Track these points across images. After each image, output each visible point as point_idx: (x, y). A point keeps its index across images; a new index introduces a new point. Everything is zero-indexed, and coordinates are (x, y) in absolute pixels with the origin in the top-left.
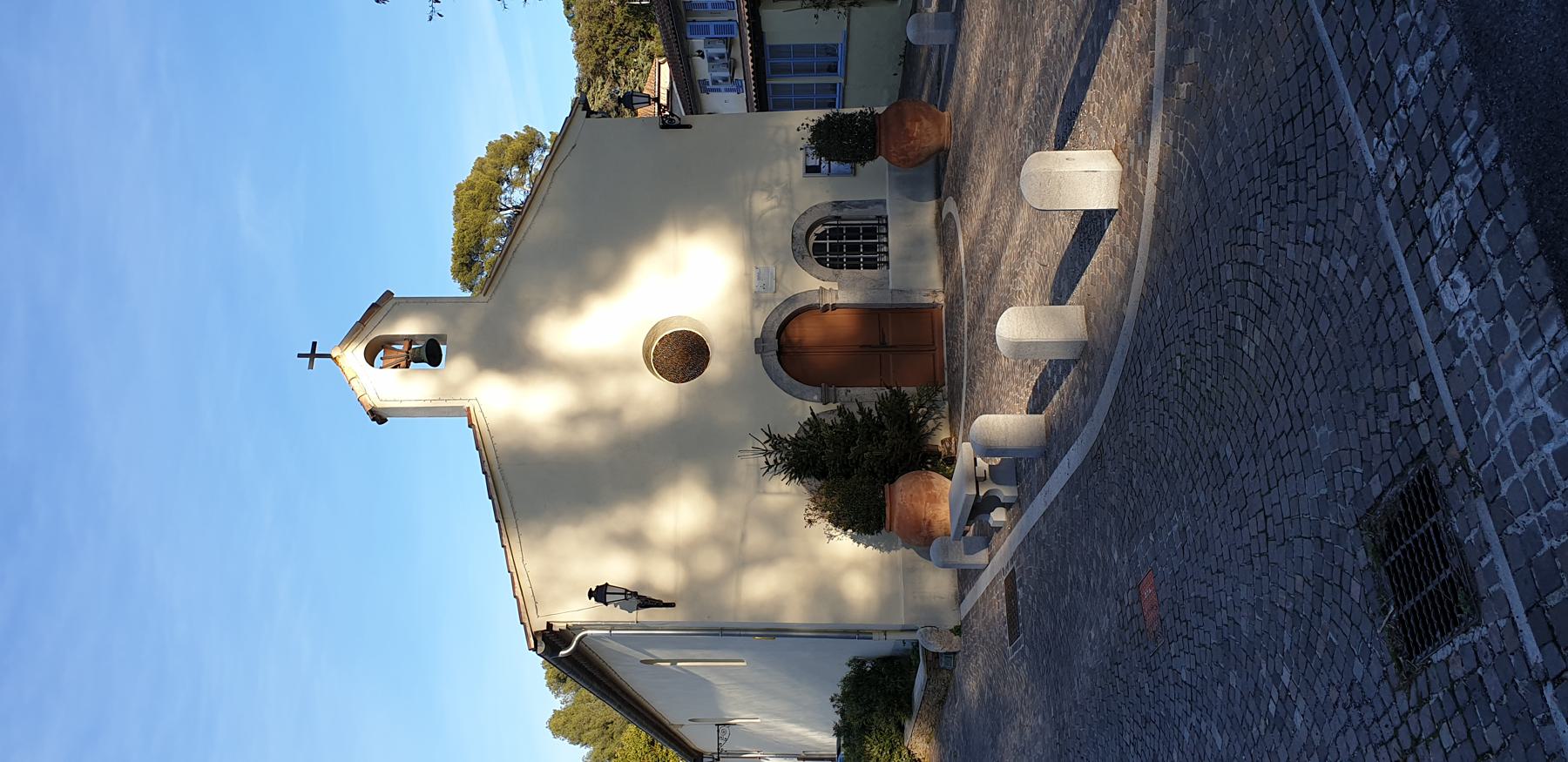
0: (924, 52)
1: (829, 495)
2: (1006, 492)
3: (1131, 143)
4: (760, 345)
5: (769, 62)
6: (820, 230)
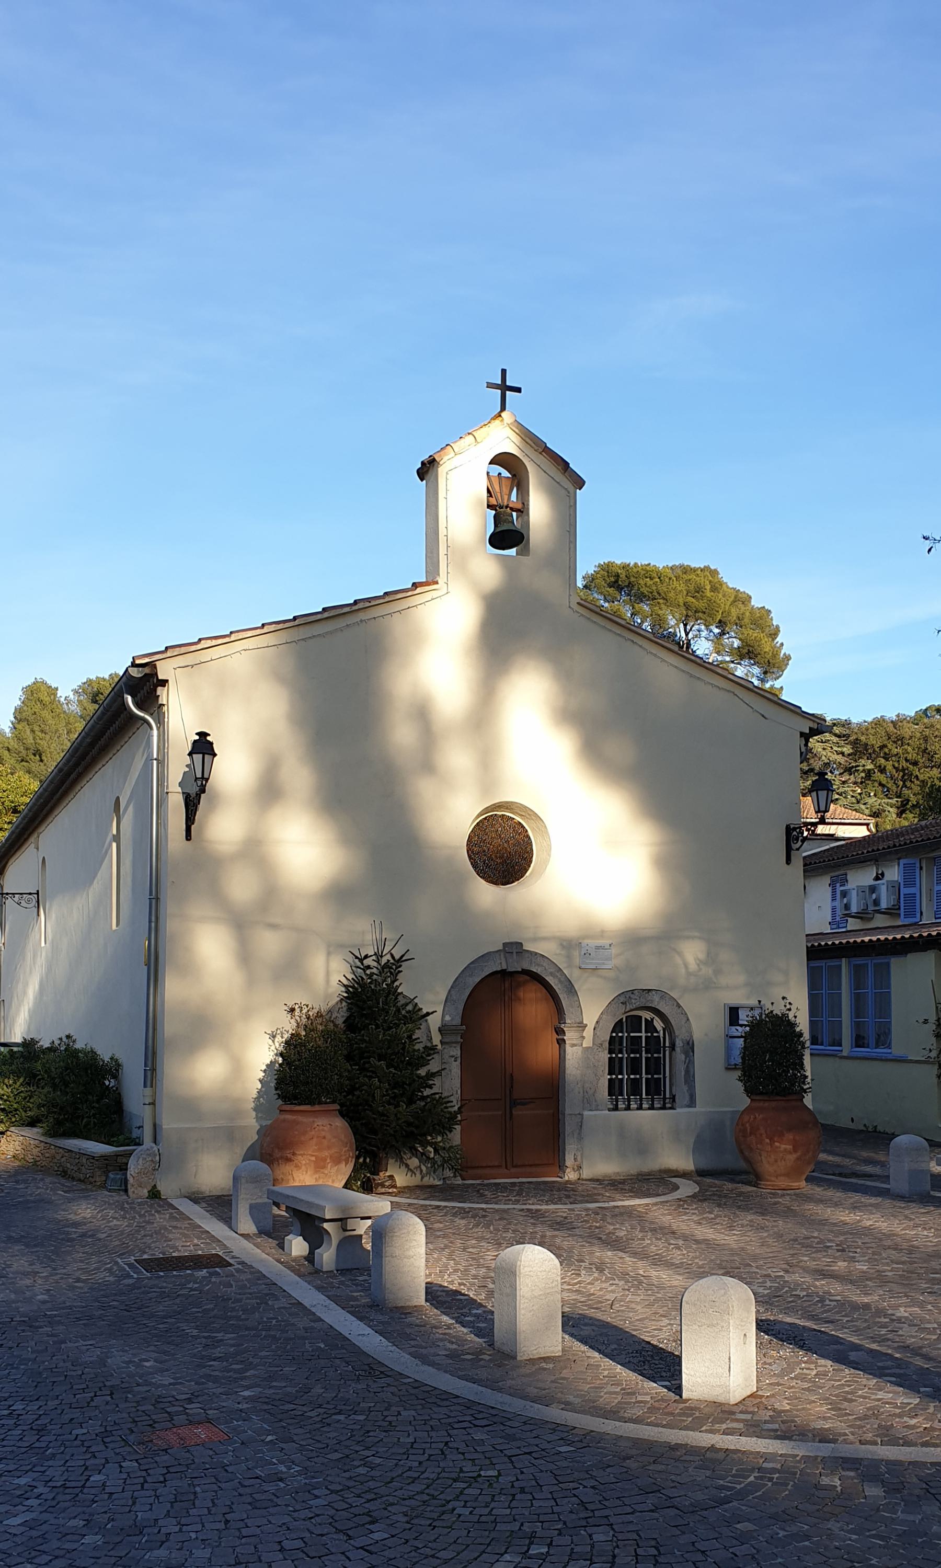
0: (881, 1157)
1: (326, 1034)
2: (327, 1256)
3: (766, 1415)
4: (514, 948)
5: (870, 962)
6: (658, 1024)
